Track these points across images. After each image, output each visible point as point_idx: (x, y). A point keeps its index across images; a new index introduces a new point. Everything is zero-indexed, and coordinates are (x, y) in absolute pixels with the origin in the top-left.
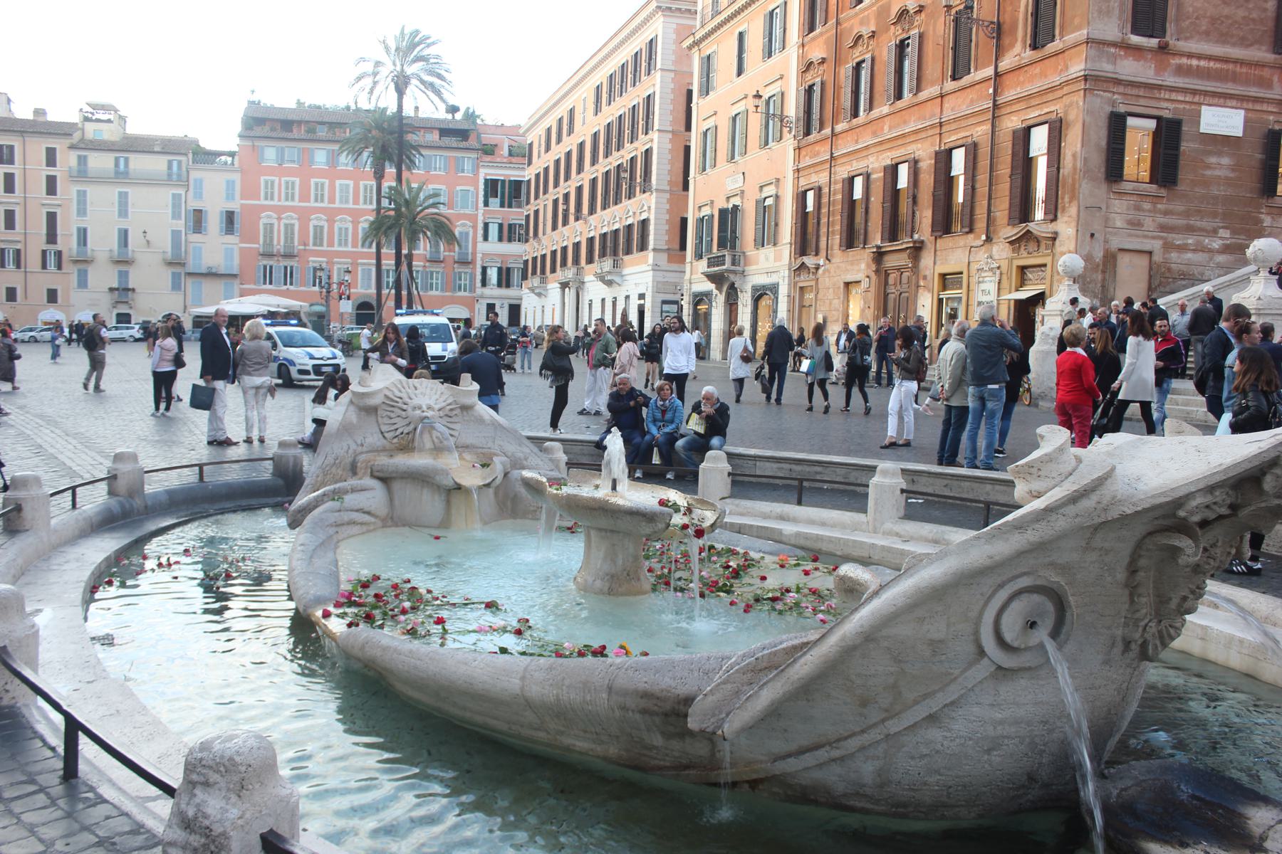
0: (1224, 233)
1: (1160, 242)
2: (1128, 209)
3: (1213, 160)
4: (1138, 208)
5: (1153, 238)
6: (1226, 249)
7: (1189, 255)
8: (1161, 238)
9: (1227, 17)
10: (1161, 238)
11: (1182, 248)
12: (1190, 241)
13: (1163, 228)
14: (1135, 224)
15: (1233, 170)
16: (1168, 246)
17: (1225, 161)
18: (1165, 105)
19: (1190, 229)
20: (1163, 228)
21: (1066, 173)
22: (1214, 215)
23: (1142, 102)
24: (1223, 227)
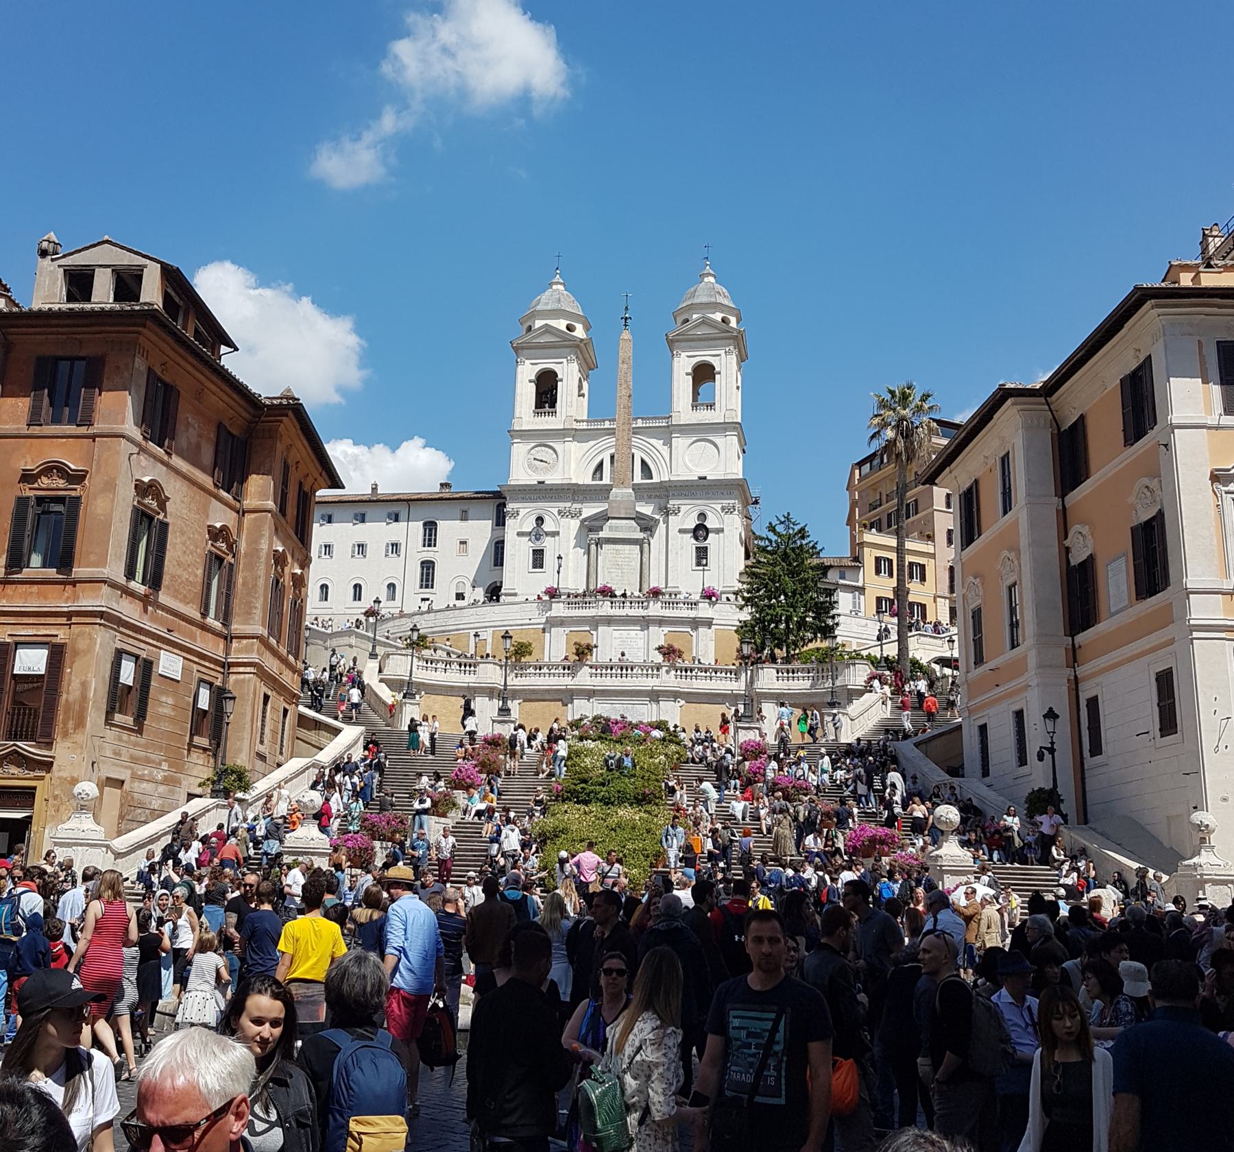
0: (165, 766)
1: (130, 772)
2: (114, 740)
3: (163, 699)
4: (120, 740)
5: (126, 767)
6: (167, 781)
7: (145, 785)
8: (132, 769)
9: (179, 577)
10: (132, 769)
11: (141, 779)
12: (146, 772)
13: (134, 760)
14: (117, 754)
15: (174, 710)
16: (135, 777)
17: (170, 701)
18: (142, 645)
19: (148, 761)
20: (134, 760)
21: (71, 698)
22: (161, 749)
23: (131, 641)
24: (165, 761)
